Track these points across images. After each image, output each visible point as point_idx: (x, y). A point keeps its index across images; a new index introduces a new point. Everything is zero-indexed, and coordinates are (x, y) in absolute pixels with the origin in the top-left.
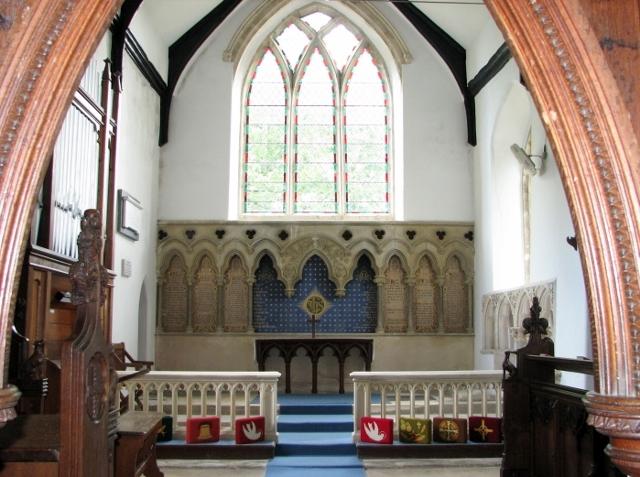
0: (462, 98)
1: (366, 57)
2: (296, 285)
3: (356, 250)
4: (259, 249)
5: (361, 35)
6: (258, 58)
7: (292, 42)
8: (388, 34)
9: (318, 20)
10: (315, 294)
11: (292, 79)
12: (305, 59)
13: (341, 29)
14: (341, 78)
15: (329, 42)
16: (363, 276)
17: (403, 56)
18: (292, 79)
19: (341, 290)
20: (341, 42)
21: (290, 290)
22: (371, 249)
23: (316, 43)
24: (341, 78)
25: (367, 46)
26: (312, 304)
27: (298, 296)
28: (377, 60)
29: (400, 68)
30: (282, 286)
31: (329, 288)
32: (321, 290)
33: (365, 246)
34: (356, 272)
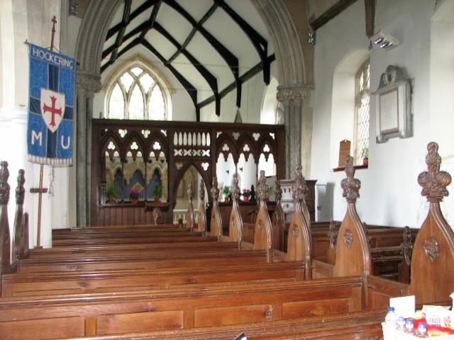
0: (194, 108)
1: (157, 88)
2: (131, 181)
3: (153, 167)
4: (117, 167)
5: (155, 79)
6: (114, 85)
7: (127, 80)
8: (167, 81)
9: (137, 71)
10: (138, 184)
11: (127, 96)
12: (132, 87)
13: (147, 75)
14: (147, 97)
15: (142, 80)
16: (156, 177)
17: (173, 91)
18: (127, 96)
19: (148, 182)
20: (147, 81)
21: (128, 182)
22: (159, 167)
23: (137, 80)
24: (147, 97)
25: (158, 83)
26: (137, 187)
27: (131, 185)
28: (161, 89)
29: (171, 94)
30: (125, 181)
31: (143, 181)
32: (140, 182)
33: (157, 166)
34: (153, 176)
